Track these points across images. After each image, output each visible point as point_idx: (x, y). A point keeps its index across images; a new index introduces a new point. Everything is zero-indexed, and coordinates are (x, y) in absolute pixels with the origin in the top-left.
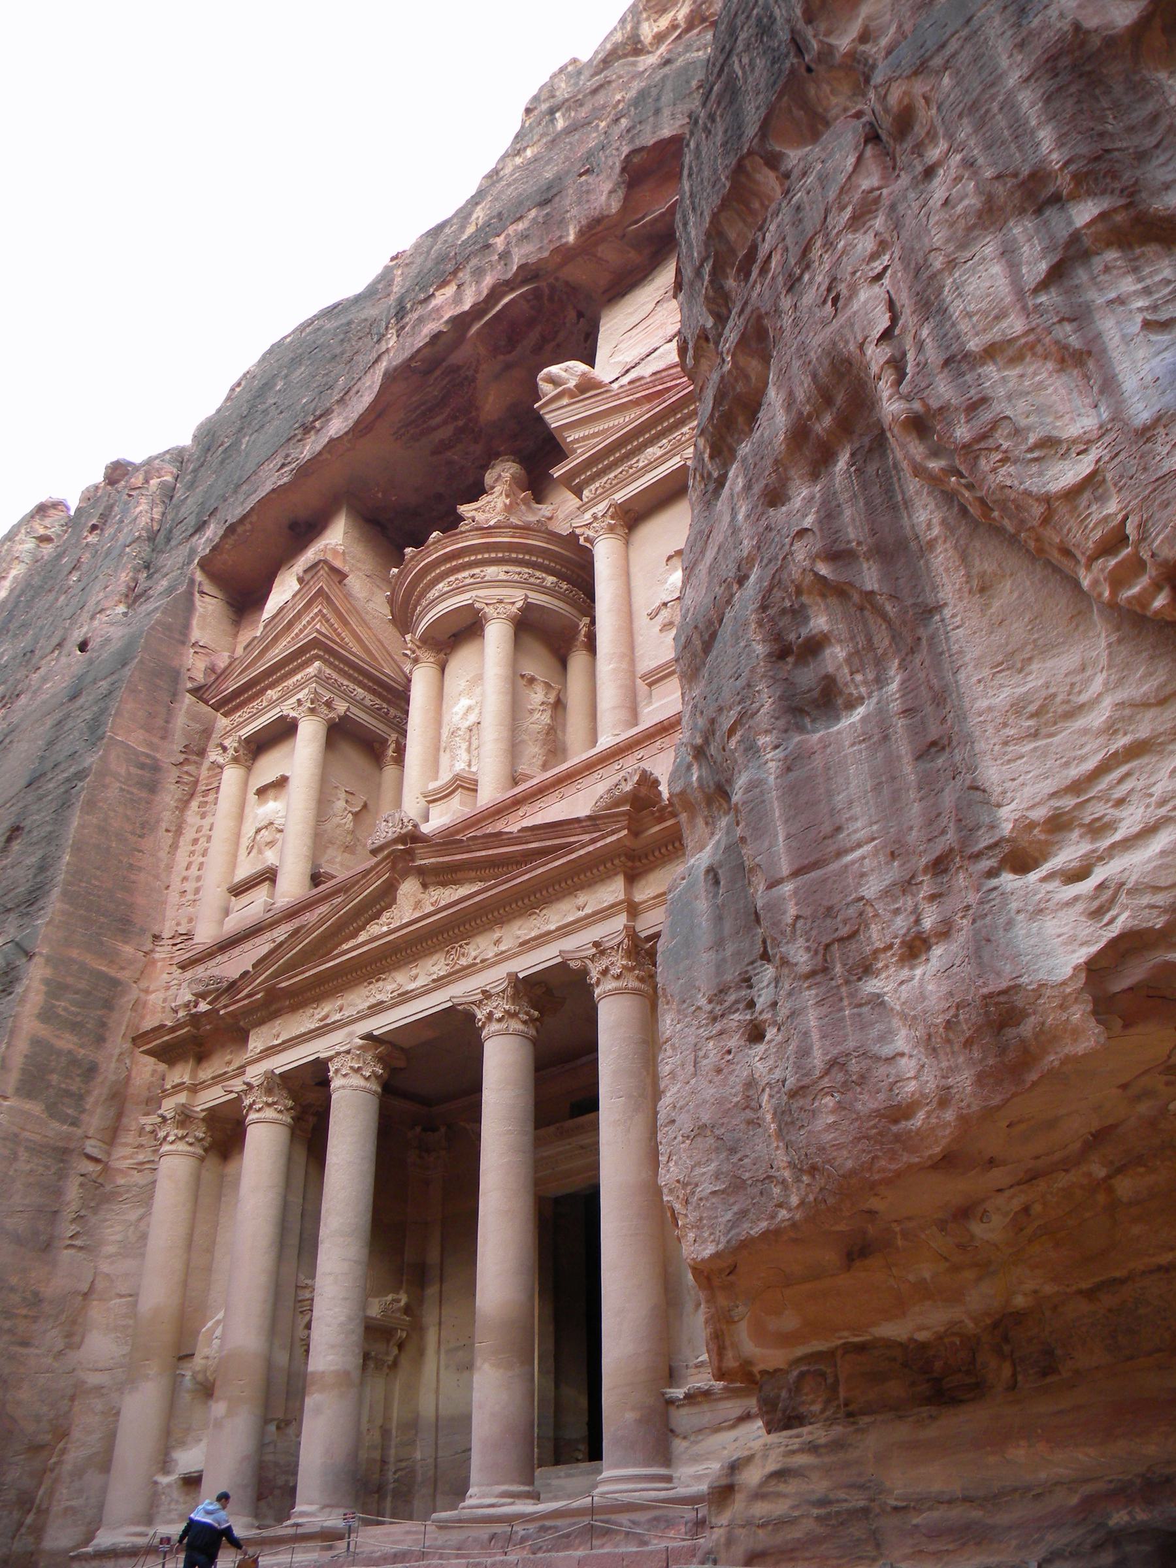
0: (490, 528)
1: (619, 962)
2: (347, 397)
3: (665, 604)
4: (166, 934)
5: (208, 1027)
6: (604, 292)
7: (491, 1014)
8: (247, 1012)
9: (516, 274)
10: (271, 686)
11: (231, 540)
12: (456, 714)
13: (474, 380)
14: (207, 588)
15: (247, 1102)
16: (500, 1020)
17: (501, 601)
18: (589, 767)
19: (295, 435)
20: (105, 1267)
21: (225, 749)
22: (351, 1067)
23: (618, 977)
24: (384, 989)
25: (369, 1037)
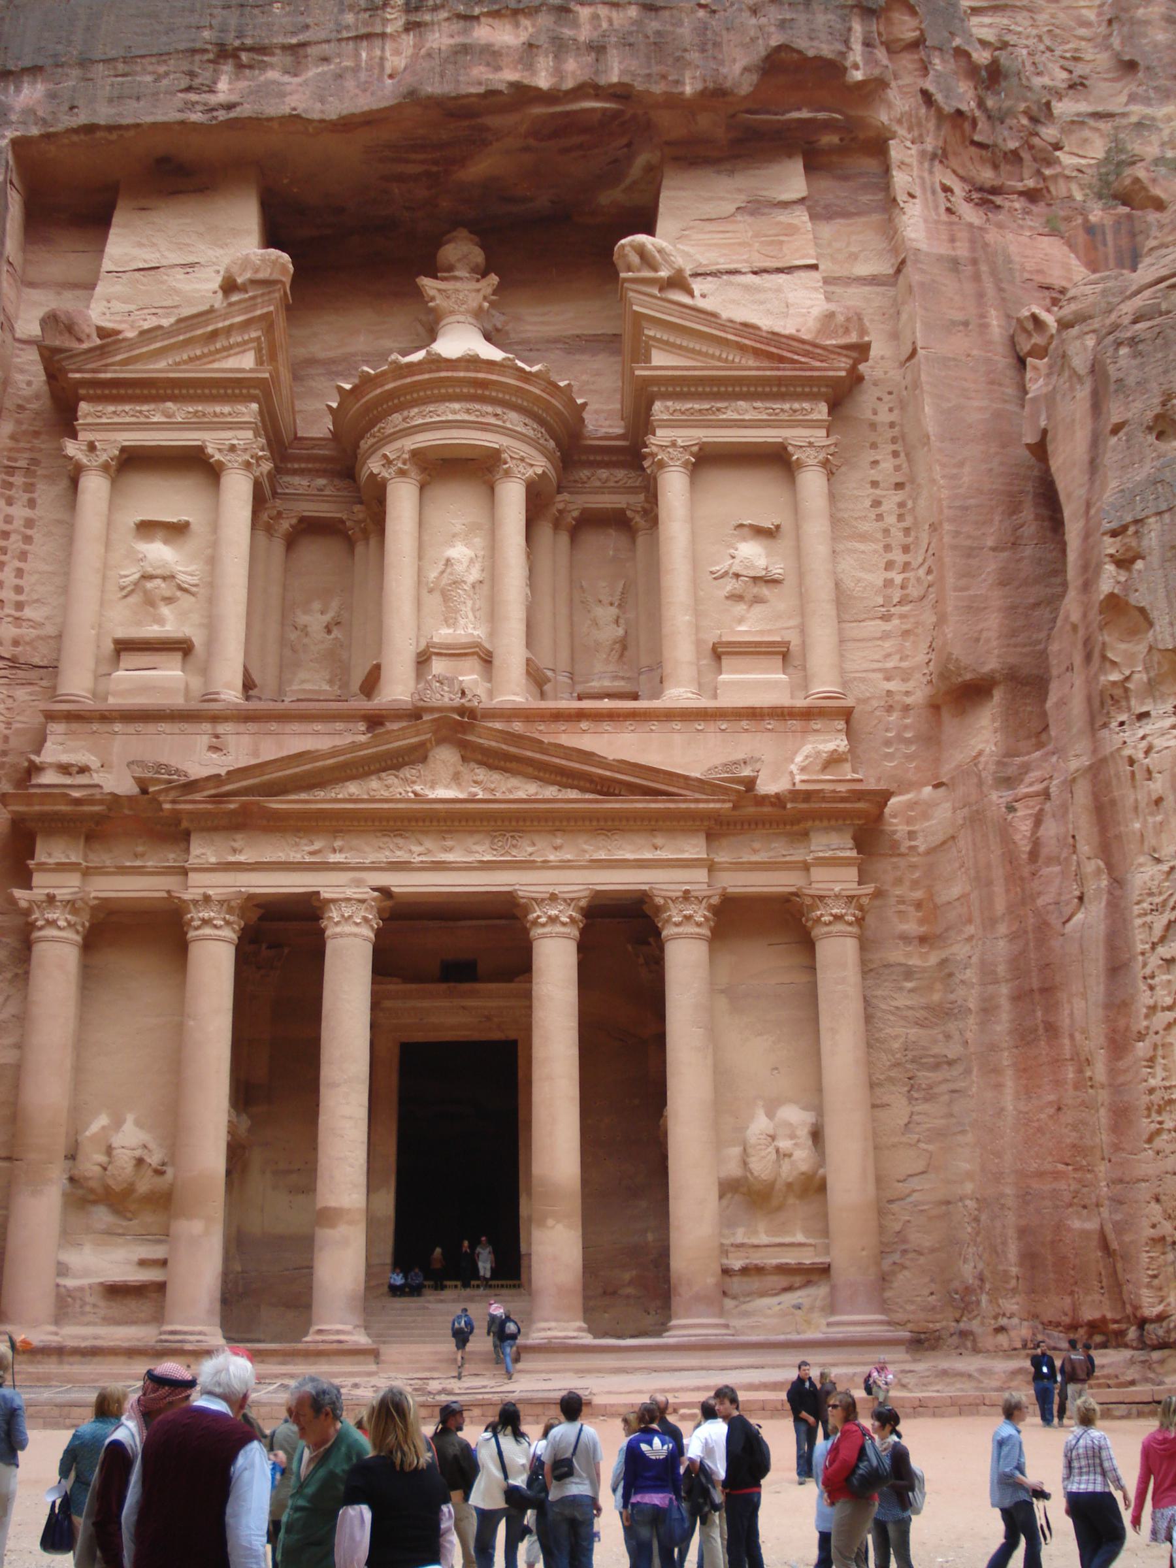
1: (700, 913)
2: (301, 52)
5: (127, 812)
6: (668, 143)
7: (557, 917)
8: (190, 813)
10: (173, 398)
11: (75, 138)
12: (460, 562)
15: (206, 915)
16: (564, 924)
17: (522, 459)
19: (205, 51)
21: (92, 447)
22: (365, 919)
23: (699, 925)
24: (415, 850)
25: (385, 892)
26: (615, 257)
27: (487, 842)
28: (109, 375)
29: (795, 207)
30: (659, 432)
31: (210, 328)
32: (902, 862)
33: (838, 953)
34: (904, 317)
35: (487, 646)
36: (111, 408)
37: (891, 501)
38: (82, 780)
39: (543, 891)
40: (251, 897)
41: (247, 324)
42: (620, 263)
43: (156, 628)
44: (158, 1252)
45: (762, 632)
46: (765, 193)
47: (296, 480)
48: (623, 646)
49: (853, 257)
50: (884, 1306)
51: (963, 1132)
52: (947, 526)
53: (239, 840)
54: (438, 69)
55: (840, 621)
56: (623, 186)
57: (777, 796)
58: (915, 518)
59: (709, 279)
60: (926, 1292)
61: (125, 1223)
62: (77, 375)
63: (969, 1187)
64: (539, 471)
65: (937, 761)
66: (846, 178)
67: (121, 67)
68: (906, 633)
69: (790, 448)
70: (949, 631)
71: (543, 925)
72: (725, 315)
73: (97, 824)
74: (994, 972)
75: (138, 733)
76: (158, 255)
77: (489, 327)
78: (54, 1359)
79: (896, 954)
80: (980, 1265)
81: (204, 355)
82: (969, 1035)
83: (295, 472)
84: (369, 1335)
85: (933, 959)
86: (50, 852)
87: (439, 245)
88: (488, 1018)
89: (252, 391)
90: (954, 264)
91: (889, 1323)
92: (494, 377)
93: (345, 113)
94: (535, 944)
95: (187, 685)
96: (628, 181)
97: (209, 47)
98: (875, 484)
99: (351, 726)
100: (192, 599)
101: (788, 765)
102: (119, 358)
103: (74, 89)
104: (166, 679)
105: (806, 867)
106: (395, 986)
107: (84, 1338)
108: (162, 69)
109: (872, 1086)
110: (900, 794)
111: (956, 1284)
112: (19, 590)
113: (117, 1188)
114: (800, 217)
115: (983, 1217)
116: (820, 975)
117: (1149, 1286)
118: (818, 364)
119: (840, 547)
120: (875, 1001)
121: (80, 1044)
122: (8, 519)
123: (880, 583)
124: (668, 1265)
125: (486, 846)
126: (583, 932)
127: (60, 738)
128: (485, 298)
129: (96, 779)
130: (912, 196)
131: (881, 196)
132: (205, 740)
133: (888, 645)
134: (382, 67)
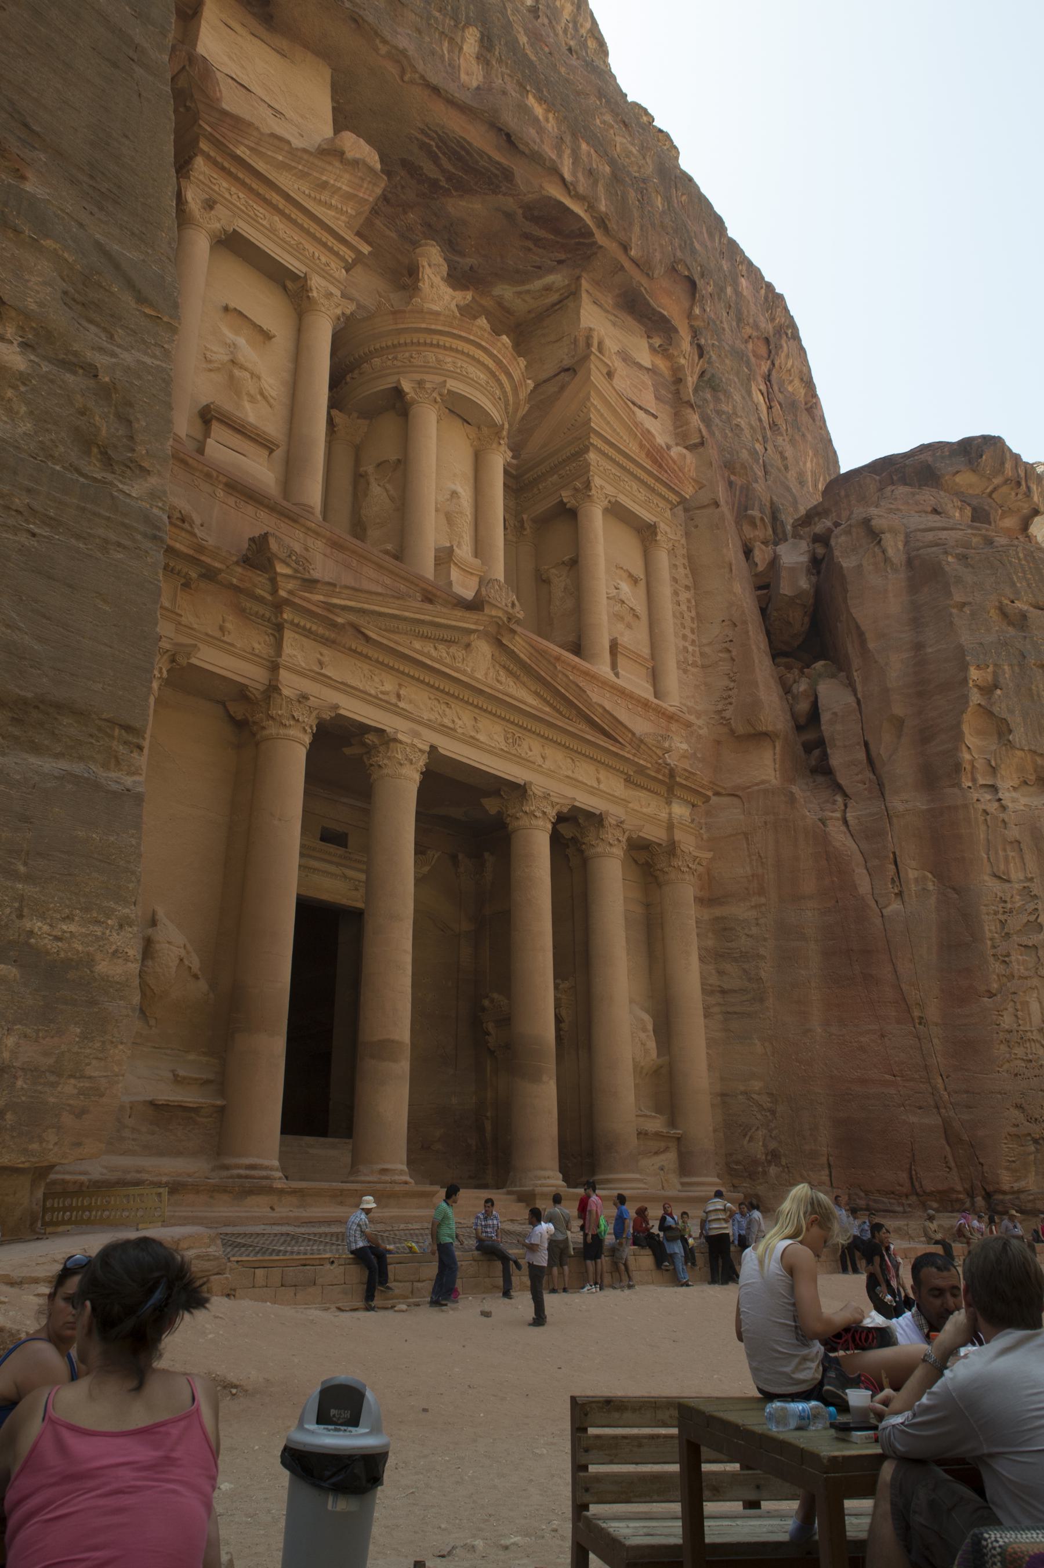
1: (624, 839)
3: (623, 602)
5: (235, 581)
18: (604, 684)
25: (433, 748)
31: (324, 178)
36: (225, 184)
37: (684, 596)
41: (349, 197)
53: (328, 654)
56: (519, 289)
58: (697, 613)
62: (209, 129)
63: (757, 1085)
80: (773, 1145)
82: (763, 974)
96: (527, 287)
104: (261, 471)
114: (646, 379)
117: (1007, 1169)
125: (501, 739)
131: (670, 396)
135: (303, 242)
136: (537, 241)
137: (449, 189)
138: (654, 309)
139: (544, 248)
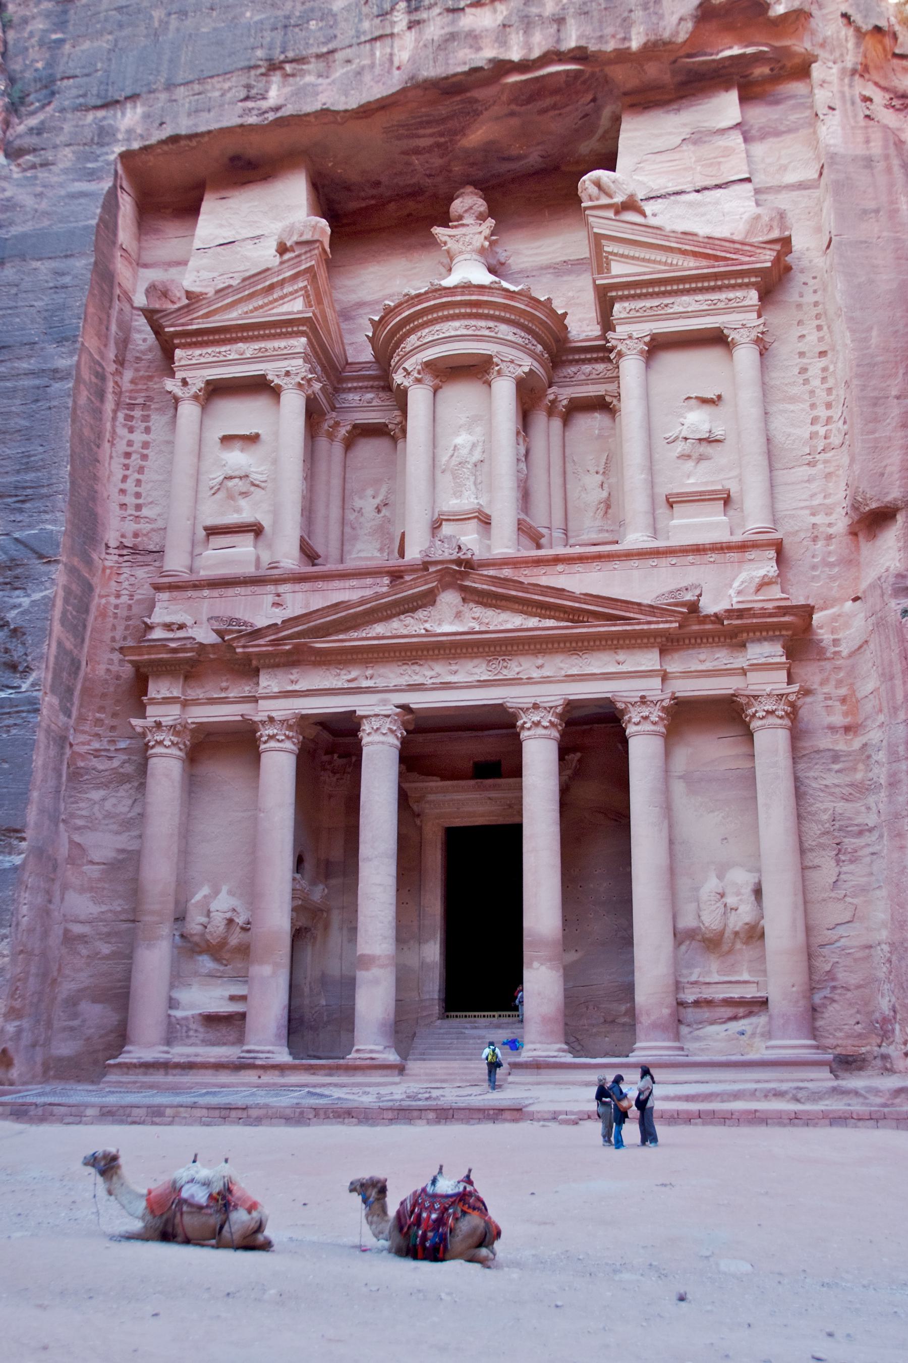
0: (514, 292)
1: (655, 714)
2: (330, 57)
3: (686, 439)
4: (113, 543)
5: (212, 656)
7: (539, 722)
9: (572, 50)
11: (165, 148)
12: (463, 446)
13: (481, 113)
14: (125, 185)
15: (271, 732)
16: (545, 728)
17: (512, 362)
18: (628, 555)
19: (257, 67)
20: (77, 838)
21: (185, 382)
22: (390, 730)
23: (655, 723)
25: (406, 708)
26: (580, 190)
27: (484, 666)
28: (194, 327)
29: (731, 132)
30: (618, 329)
31: (268, 283)
32: (828, 665)
33: (771, 740)
34: (825, 211)
35: (488, 512)
36: (198, 352)
37: (816, 367)
38: (181, 634)
39: (528, 702)
40: (304, 717)
41: (295, 277)
42: (583, 195)
43: (235, 516)
44: (238, 990)
45: (706, 483)
46: (706, 124)
47: (350, 396)
48: (607, 504)
49: (783, 168)
50: (814, 1033)
51: (879, 887)
52: (855, 382)
53: (295, 674)
54: (431, 56)
55: (771, 469)
56: (597, 136)
57: (716, 615)
59: (660, 200)
60: (853, 1022)
61: (222, 968)
62: (172, 329)
63: (884, 934)
64: (527, 369)
65: (857, 578)
66: (777, 102)
67: (197, 87)
68: (828, 476)
69: (725, 331)
70: (856, 467)
71: (529, 729)
72: (668, 228)
73: (192, 665)
74: (897, 752)
75: (221, 596)
76: (233, 232)
77: (493, 262)
78: (162, 1071)
79: (825, 742)
81: (266, 305)
82: (881, 806)
83: (350, 390)
84: (399, 1054)
85: (857, 744)
86: (158, 689)
87: (451, 199)
88: (510, 806)
89: (301, 328)
90: (868, 162)
91: (817, 1047)
92: (485, 298)
93: (363, 101)
94: (524, 744)
95: (258, 559)
97: (260, 63)
98: (802, 354)
99: (378, 580)
100: (263, 492)
101: (726, 589)
102: (201, 313)
103: (163, 109)
104: (241, 555)
105: (744, 672)
106: (435, 783)
107: (188, 1056)
108: (226, 85)
109: (803, 852)
110: (826, 609)
111: (877, 1015)
112: (138, 495)
113: (214, 942)
114: (736, 139)
115: (894, 958)
116: (758, 761)
118: (747, 259)
119: (772, 409)
120: (807, 781)
121: (186, 834)
122: (130, 443)
123: (807, 435)
124: (633, 999)
126: (563, 734)
127: (166, 604)
128: (486, 238)
129: (190, 633)
130: (833, 109)
131: (808, 113)
132: (270, 599)
133: (815, 486)
134: (391, 61)
135: (262, 344)
136: (554, 107)
137: (451, 141)
138: (714, 61)
139: (568, 105)
